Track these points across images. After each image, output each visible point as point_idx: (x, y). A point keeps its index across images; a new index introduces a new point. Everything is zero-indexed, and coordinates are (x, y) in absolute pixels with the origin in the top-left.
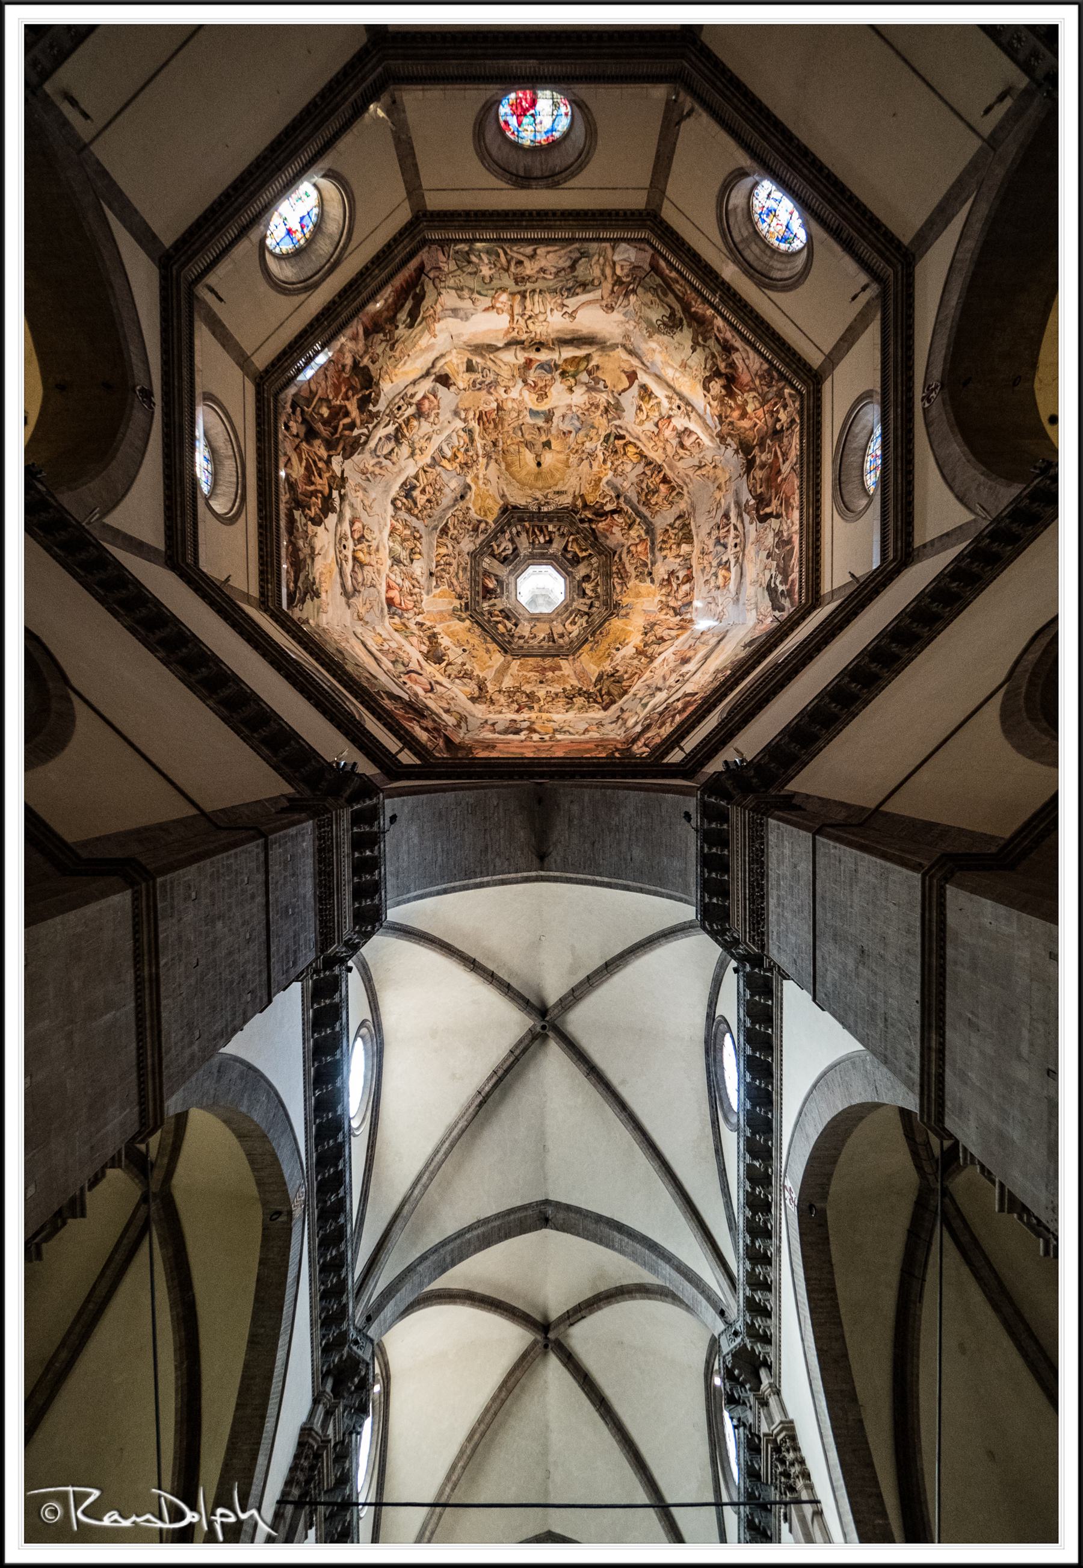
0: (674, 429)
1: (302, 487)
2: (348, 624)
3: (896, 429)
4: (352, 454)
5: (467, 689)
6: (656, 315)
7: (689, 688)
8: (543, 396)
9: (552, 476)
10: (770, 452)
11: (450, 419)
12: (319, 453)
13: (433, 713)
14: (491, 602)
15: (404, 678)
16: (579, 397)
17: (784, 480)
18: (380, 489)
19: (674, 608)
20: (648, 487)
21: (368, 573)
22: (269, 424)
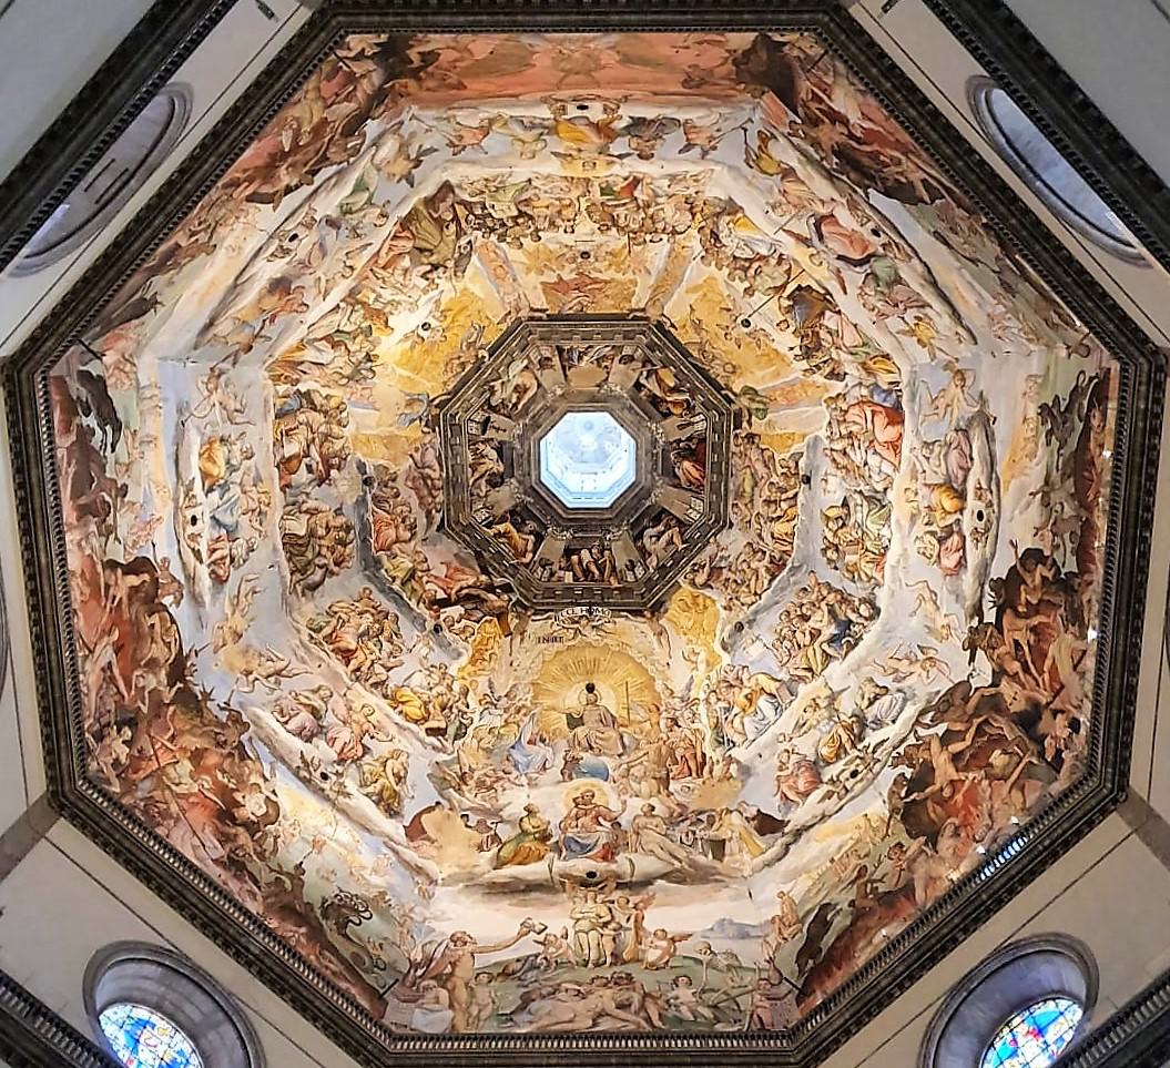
1: (1056, 618)
4: (951, 691)
6: (373, 927)
7: (266, 218)
8: (583, 803)
9: (565, 667)
12: (1017, 687)
13: (817, 165)
15: (876, 243)
22: (1108, 719)
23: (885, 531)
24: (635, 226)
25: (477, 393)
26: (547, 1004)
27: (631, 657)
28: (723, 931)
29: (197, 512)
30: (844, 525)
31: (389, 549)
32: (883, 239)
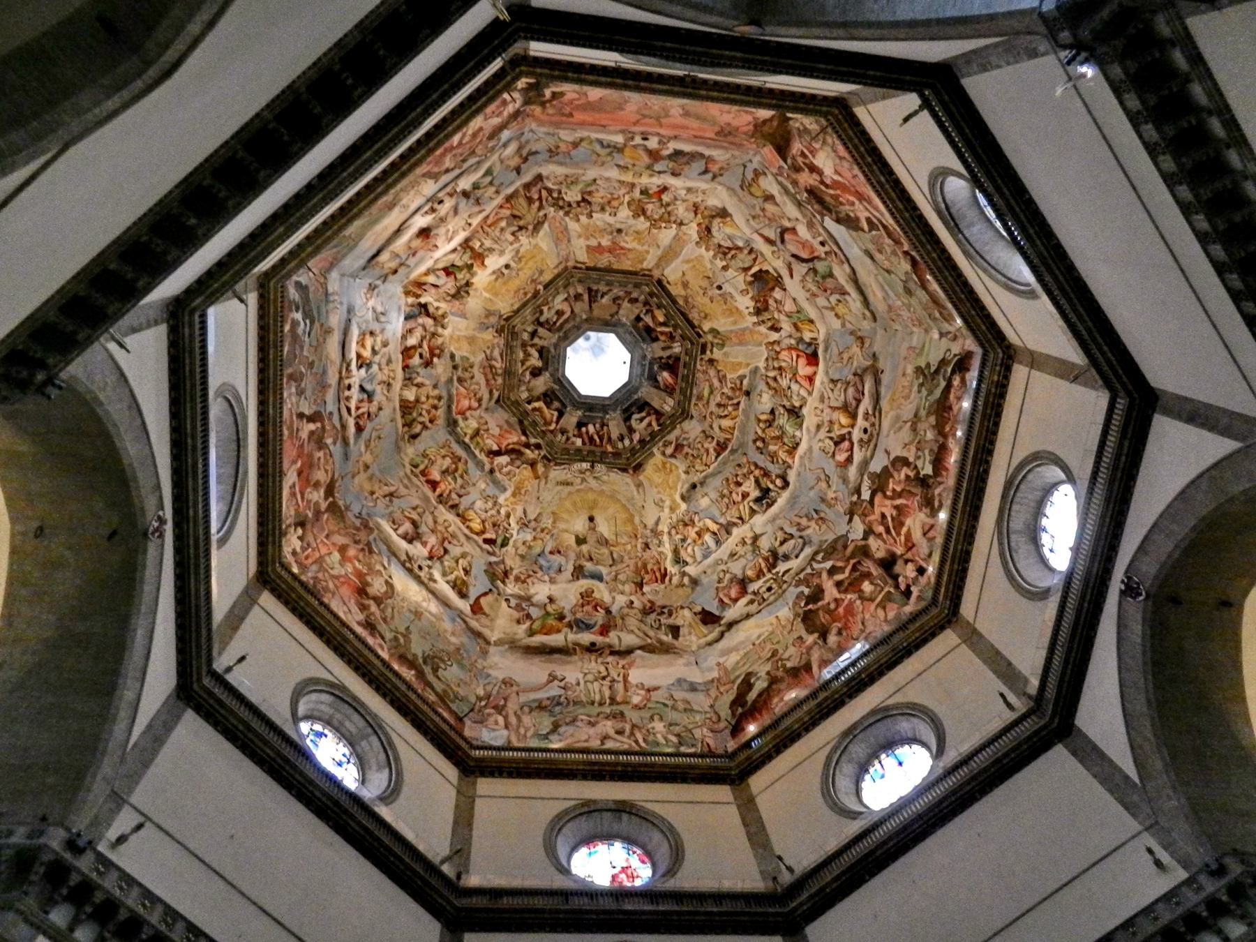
0: (424, 544)
1: (915, 502)
2: (880, 332)
3: (195, 490)
4: (836, 541)
7: (429, 188)
8: (586, 596)
9: (574, 504)
10: (309, 502)
11: (703, 576)
12: (880, 542)
13: (793, 197)
14: (668, 353)
15: (821, 251)
16: (541, 591)
17: (294, 462)
18: (803, 499)
19: (428, 315)
20: (455, 479)
21: (837, 398)
23: (798, 433)
24: (656, 217)
26: (570, 729)
27: (619, 500)
29: (351, 381)
30: (770, 426)
31: (462, 413)
32: (827, 248)
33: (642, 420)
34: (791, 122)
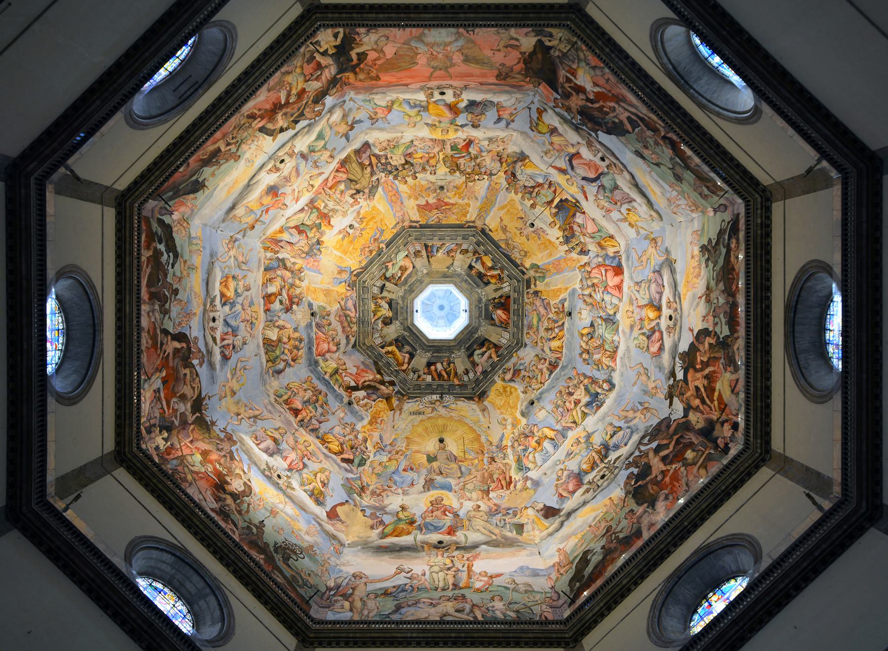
0: (285, 458)
2: (668, 228)
4: (659, 424)
5: (529, 171)
8: (436, 504)
9: (426, 429)
11: (544, 478)
14: (497, 295)
17: (161, 371)
19: (286, 268)
24: (469, 170)
25: (378, 269)
27: (466, 424)
28: (523, 572)
29: (216, 315)
30: (592, 337)
31: (323, 355)
32: (607, 162)
33: (483, 354)
34: (552, 52)
